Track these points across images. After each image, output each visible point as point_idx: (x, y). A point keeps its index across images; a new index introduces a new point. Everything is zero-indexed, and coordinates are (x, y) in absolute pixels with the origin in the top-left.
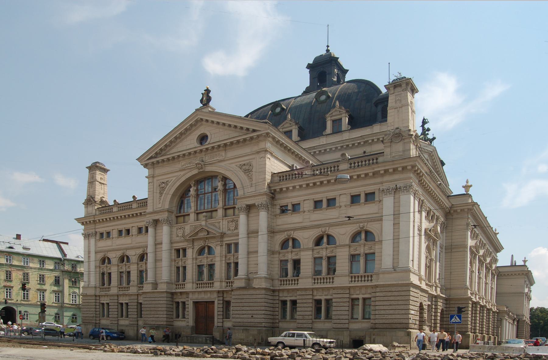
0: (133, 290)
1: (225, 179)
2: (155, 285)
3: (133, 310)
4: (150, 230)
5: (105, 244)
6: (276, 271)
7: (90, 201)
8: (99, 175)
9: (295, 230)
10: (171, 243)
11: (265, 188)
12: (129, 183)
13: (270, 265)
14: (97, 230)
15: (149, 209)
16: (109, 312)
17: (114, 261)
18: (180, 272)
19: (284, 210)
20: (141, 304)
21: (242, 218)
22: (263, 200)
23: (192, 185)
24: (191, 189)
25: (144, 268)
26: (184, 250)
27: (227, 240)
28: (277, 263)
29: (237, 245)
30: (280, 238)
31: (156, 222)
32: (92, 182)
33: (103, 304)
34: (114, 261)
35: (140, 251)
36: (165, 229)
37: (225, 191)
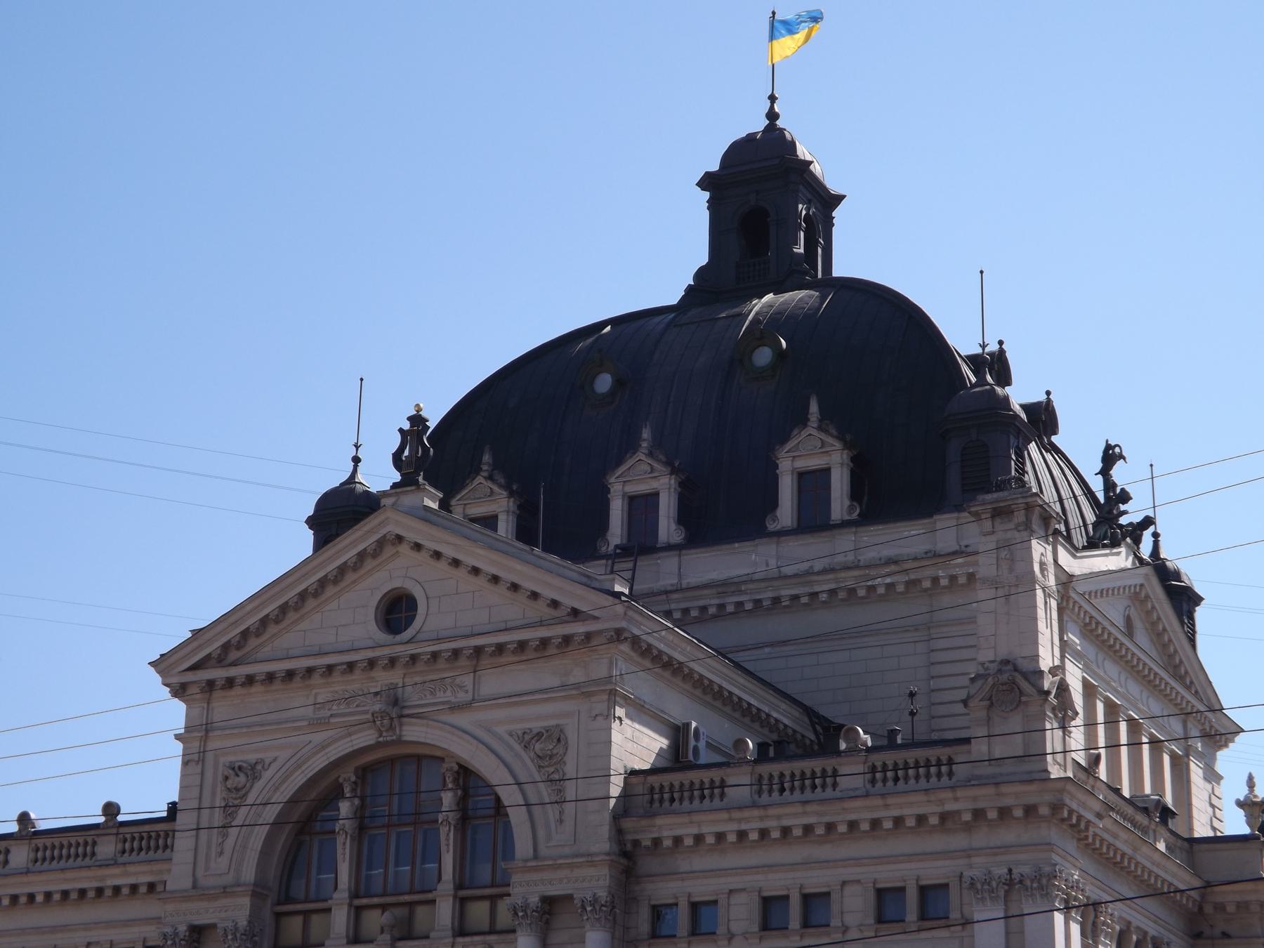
1: (465, 774)
11: (600, 840)
15: (178, 875)
22: (595, 882)
23: (347, 791)
24: (345, 808)
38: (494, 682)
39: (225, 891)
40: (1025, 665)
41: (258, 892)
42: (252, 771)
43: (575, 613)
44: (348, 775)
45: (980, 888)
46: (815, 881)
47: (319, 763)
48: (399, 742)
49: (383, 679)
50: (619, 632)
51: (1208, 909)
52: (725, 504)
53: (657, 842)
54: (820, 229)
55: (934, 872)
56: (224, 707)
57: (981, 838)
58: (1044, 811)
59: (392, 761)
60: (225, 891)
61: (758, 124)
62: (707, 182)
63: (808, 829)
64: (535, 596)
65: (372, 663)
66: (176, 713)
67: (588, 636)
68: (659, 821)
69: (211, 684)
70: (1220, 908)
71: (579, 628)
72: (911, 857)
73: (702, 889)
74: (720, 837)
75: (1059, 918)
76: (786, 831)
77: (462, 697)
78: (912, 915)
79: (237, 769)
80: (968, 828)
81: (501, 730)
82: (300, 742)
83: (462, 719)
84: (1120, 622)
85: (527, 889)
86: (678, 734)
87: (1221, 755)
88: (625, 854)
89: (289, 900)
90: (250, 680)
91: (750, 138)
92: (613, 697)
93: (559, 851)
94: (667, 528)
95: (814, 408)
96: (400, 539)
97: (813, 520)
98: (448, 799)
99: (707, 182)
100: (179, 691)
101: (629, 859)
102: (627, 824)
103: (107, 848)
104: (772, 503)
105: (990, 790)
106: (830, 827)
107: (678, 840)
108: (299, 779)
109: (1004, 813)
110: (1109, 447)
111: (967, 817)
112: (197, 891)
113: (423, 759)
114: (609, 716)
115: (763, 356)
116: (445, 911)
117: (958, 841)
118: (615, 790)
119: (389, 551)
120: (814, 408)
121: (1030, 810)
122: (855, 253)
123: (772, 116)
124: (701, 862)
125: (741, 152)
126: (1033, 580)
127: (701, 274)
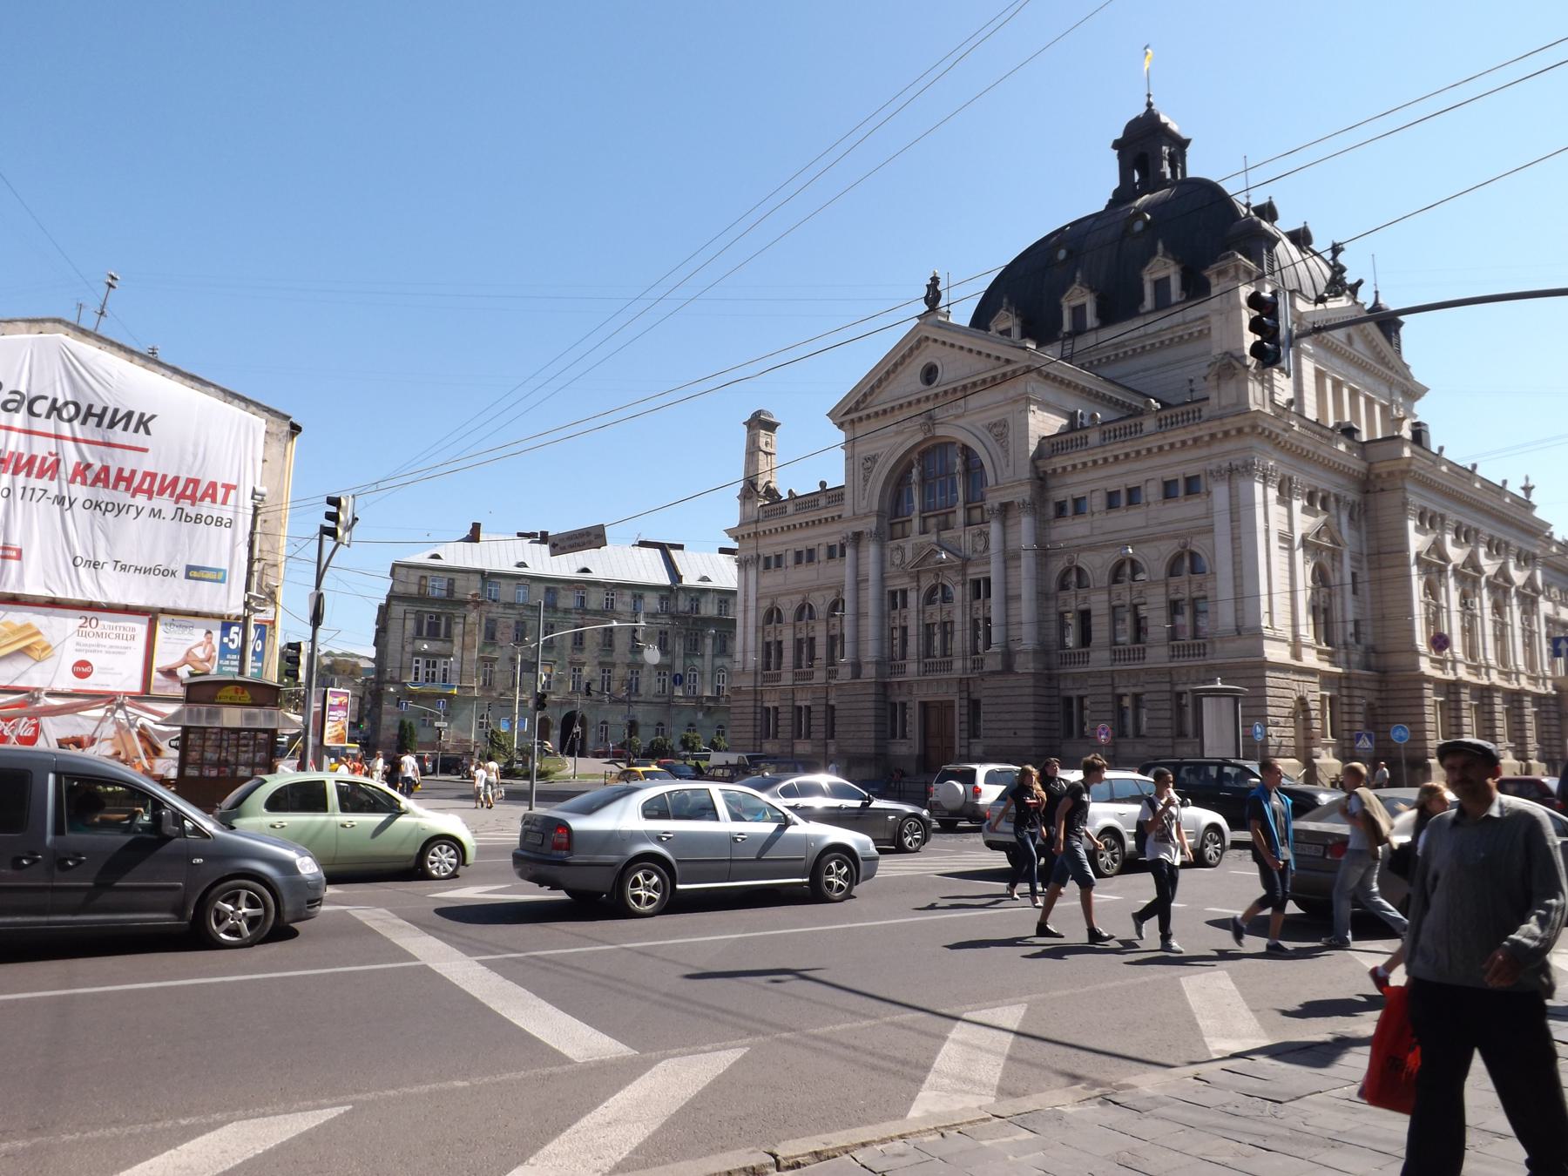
0: (820, 676)
1: (966, 449)
2: (857, 668)
3: (818, 721)
4: (848, 552)
5: (773, 580)
8: (763, 437)
9: (1080, 549)
10: (883, 579)
11: (1025, 473)
12: (812, 460)
14: (761, 552)
15: (847, 510)
16: (776, 726)
17: (789, 614)
19: (1061, 509)
20: (833, 707)
21: (994, 529)
22: (1024, 493)
24: (914, 471)
25: (836, 632)
26: (904, 592)
27: (974, 572)
29: (988, 581)
30: (1058, 565)
31: (858, 536)
33: (768, 709)
34: (789, 614)
35: (831, 596)
36: (871, 551)
37: (967, 471)
38: (975, 401)
39: (866, 516)
40: (1237, 354)
41: (880, 514)
42: (873, 459)
43: (1008, 361)
44: (915, 456)
45: (1217, 475)
46: (1132, 481)
47: (901, 452)
48: (934, 437)
49: (925, 407)
52: (1118, 304)
53: (1054, 470)
54: (1178, 158)
55: (1192, 470)
56: (861, 429)
57: (1216, 448)
58: (1247, 430)
59: (935, 446)
60: (866, 516)
61: (1142, 110)
62: (1117, 145)
63: (1127, 455)
64: (988, 356)
65: (919, 401)
66: (840, 436)
67: (1014, 371)
68: (1054, 460)
69: (852, 421)
70: (1378, 476)
71: (1009, 368)
72: (1179, 463)
73: (1078, 492)
74: (1085, 464)
75: (1258, 487)
76: (1116, 458)
77: (960, 411)
78: (1181, 493)
79: (867, 459)
80: (1208, 444)
82: (894, 442)
83: (961, 422)
84: (1344, 339)
85: (993, 500)
86: (1072, 416)
87: (1417, 404)
88: (1041, 479)
89: (896, 516)
90: (868, 417)
91: (1137, 119)
92: (1028, 401)
93: (1008, 481)
94: (1091, 320)
95: (1160, 246)
96: (927, 338)
97: (1162, 303)
98: (958, 461)
99: (1117, 145)
100: (841, 426)
101: (1041, 480)
102: (1040, 463)
103: (823, 502)
104: (1142, 299)
105: (1217, 423)
106: (1138, 453)
107: (1064, 469)
109: (1226, 434)
112: (855, 517)
113: (946, 445)
114: (1026, 410)
115: (1139, 226)
116: (960, 515)
117: (1204, 452)
118: (1032, 448)
119: (924, 345)
120: (1160, 246)
121: (1240, 431)
122: (1197, 166)
123: (1149, 105)
124: (1076, 478)
127: (1116, 192)
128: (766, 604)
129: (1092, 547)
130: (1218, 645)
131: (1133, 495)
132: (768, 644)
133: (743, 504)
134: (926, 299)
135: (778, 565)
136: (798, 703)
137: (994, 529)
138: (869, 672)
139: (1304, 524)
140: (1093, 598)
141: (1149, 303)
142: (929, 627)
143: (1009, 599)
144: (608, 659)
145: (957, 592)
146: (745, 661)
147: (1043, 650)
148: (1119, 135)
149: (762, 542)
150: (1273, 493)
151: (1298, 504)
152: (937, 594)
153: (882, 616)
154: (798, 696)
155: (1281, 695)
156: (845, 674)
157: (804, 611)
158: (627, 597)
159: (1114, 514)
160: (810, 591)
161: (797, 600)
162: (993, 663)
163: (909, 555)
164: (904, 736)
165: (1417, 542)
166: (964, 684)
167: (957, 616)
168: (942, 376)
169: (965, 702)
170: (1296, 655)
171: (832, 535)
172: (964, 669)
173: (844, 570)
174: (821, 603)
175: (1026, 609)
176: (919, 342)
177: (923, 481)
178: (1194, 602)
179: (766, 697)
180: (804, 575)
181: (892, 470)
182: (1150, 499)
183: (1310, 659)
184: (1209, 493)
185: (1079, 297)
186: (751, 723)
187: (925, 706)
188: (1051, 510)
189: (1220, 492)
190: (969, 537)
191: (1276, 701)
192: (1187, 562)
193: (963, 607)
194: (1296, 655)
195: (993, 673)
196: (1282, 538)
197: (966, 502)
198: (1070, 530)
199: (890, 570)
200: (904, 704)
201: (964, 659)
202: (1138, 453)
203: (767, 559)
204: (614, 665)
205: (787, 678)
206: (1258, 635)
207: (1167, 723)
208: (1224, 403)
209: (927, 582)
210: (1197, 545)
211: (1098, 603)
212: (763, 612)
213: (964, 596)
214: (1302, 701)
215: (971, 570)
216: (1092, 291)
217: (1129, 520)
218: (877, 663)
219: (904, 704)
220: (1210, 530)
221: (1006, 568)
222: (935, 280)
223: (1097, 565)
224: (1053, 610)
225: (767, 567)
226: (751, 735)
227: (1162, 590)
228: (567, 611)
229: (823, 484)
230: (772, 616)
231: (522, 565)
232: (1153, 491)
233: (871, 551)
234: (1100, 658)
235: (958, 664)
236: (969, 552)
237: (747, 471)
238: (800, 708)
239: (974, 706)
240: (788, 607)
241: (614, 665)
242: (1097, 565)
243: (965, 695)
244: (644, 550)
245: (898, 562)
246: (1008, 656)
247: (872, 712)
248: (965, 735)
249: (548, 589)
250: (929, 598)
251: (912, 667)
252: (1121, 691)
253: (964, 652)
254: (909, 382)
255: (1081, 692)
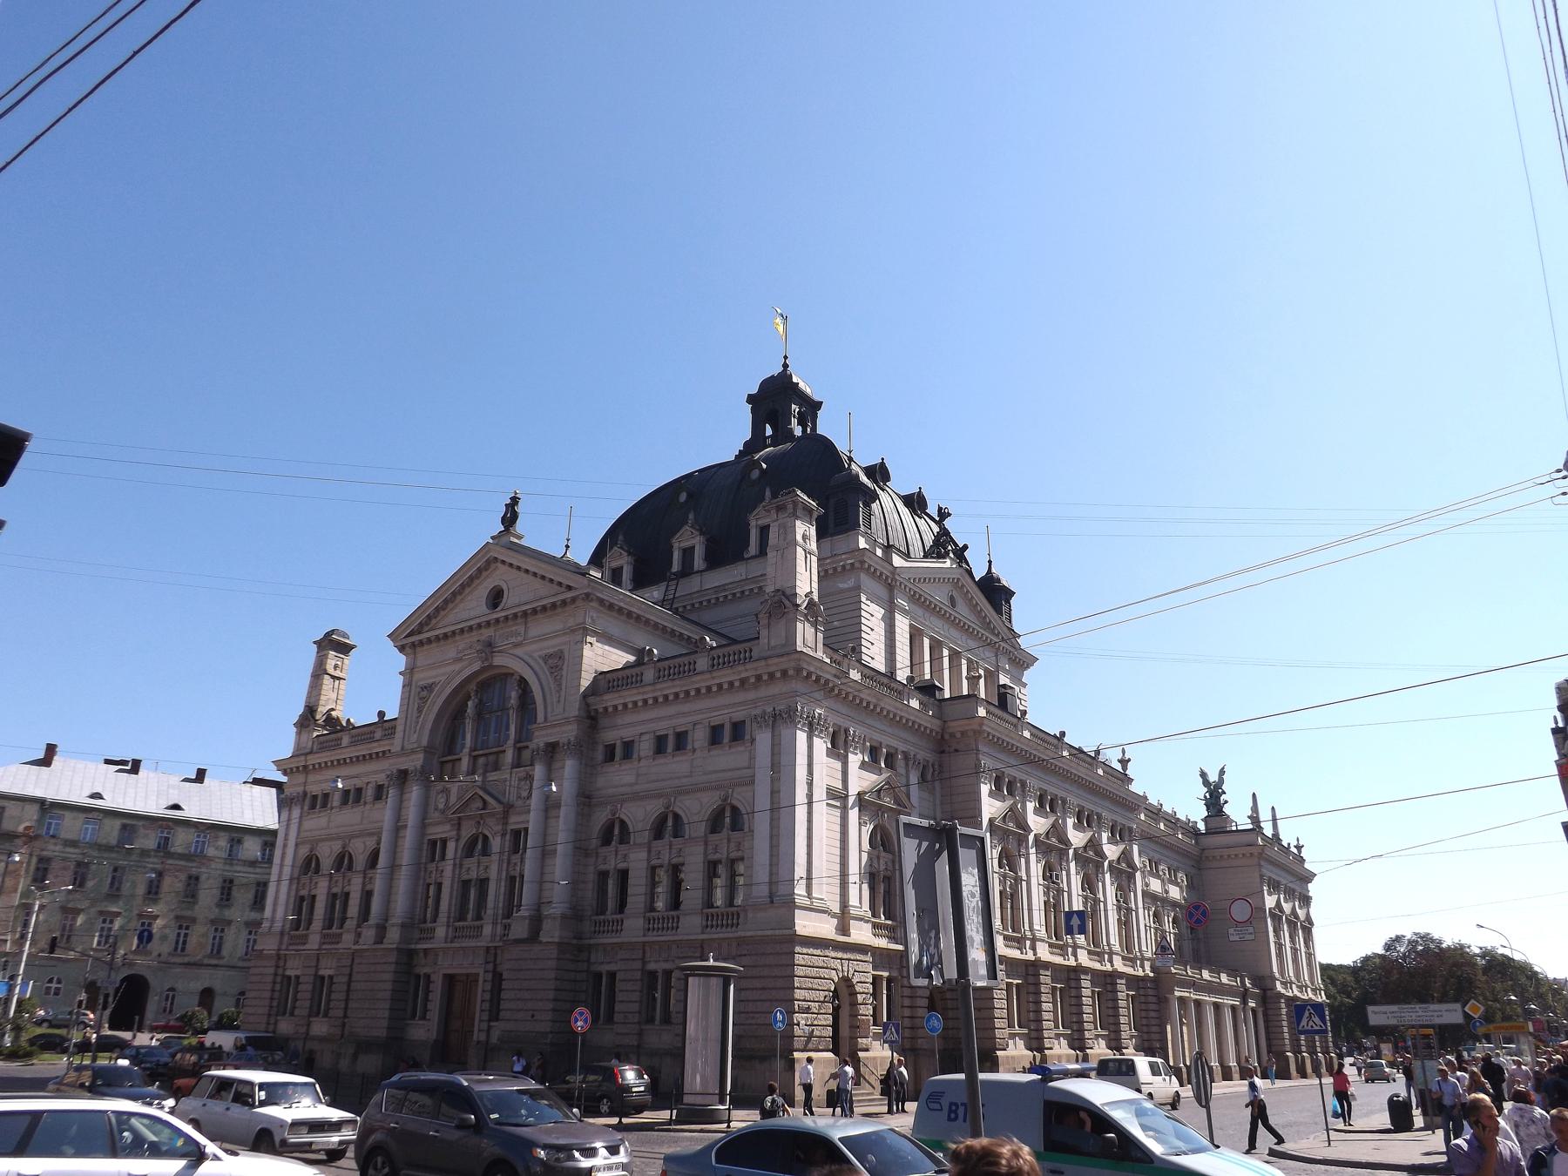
1: (523, 682)
5: (317, 823)
6: (589, 893)
7: (307, 718)
8: (332, 659)
10: (423, 825)
11: (574, 709)
13: (575, 883)
17: (327, 863)
18: (426, 893)
21: (538, 771)
24: (470, 703)
26: (444, 842)
27: (515, 821)
28: (591, 876)
30: (601, 817)
31: (403, 777)
32: (319, 672)
34: (327, 863)
36: (414, 793)
39: (413, 751)
40: (788, 592)
41: (429, 750)
42: (429, 688)
43: (569, 588)
44: (473, 686)
48: (491, 667)
50: (587, 595)
51: (947, 737)
53: (606, 709)
56: (424, 657)
57: (764, 692)
58: (791, 672)
59: (494, 677)
60: (413, 751)
62: (751, 399)
63: (676, 695)
64: (551, 581)
65: (479, 626)
66: (401, 661)
68: (606, 697)
70: (952, 735)
73: (627, 734)
74: (635, 703)
75: (801, 737)
76: (666, 697)
78: (726, 740)
79: (424, 688)
81: (536, 655)
82: (452, 667)
83: (519, 651)
85: (540, 739)
86: (641, 653)
89: (450, 754)
92: (586, 632)
94: (698, 562)
98: (514, 694)
99: (751, 399)
100: (402, 649)
101: (592, 719)
102: (591, 700)
105: (763, 663)
106: (687, 693)
107: (615, 707)
108: (448, 690)
109: (771, 676)
110: (940, 509)
111: (753, 680)
112: (404, 752)
113: (505, 676)
114: (582, 642)
115: (755, 474)
116: (509, 756)
117: (752, 695)
118: (586, 681)
119: (493, 566)
121: (784, 673)
123: (785, 366)
125: (768, 384)
126: (795, 544)
128: (304, 851)
129: (637, 797)
130: (750, 915)
131: (681, 740)
132: (302, 899)
133: (299, 734)
134: (503, 519)
135: (324, 805)
136: (321, 972)
137: (538, 771)
138: (393, 935)
139: (861, 780)
140: (632, 856)
141: (753, 549)
142: (466, 884)
143: (546, 853)
144: (188, 913)
145: (496, 844)
146: (273, 920)
147: (575, 915)
148: (755, 390)
149: (311, 778)
150: (821, 745)
151: (855, 760)
152: (476, 846)
153: (418, 868)
154: (323, 963)
155: (812, 979)
156: (369, 934)
157: (343, 861)
158: (223, 842)
159: (661, 760)
160: (352, 837)
161: (337, 847)
162: (519, 930)
163: (453, 799)
164: (423, 1018)
165: (991, 807)
166: (491, 953)
167: (493, 873)
168: (510, 600)
169: (490, 976)
170: (844, 929)
171: (375, 773)
172: (493, 935)
173: (384, 814)
174: (360, 850)
175: (559, 868)
176: (488, 563)
177: (479, 715)
178: (732, 862)
179: (290, 964)
180: (346, 819)
181: (447, 701)
182: (697, 745)
183: (862, 934)
184: (753, 740)
185: (689, 539)
186: (268, 995)
187: (450, 980)
188: (599, 755)
189: (763, 739)
190: (515, 783)
191: (808, 983)
192: (728, 819)
193: (501, 861)
194: (844, 929)
195: (518, 942)
196: (832, 794)
197: (518, 741)
198: (618, 778)
199: (434, 816)
200: (428, 976)
201: (494, 923)
202: (687, 693)
203: (315, 797)
204: (194, 920)
205: (314, 941)
206: (790, 905)
207: (635, 1007)
208: (773, 643)
209: (468, 831)
210: (739, 798)
211: (637, 862)
212: (300, 862)
213: (502, 846)
214: (846, 981)
215: (513, 819)
216: (702, 533)
217: (675, 766)
218: (403, 926)
219: (428, 976)
220: (751, 781)
221: (547, 818)
222: (515, 500)
223: (640, 816)
224: (591, 869)
225: (313, 807)
226: (266, 1010)
227: (701, 849)
228: (144, 853)
229: (381, 714)
230: (310, 865)
231: (176, 807)
232: (700, 737)
233: (414, 793)
234: (633, 927)
235: (487, 930)
236: (513, 798)
237: (309, 696)
238: (323, 978)
239: (498, 978)
240: (327, 853)
241: (194, 920)
242: (640, 816)
243: (490, 967)
244: (257, 788)
245: (441, 806)
246: (537, 921)
247: (389, 986)
248: (485, 1017)
249: (124, 827)
250: (469, 850)
251: (441, 932)
252: (651, 966)
253: (495, 915)
254: (474, 606)
255: (612, 967)
